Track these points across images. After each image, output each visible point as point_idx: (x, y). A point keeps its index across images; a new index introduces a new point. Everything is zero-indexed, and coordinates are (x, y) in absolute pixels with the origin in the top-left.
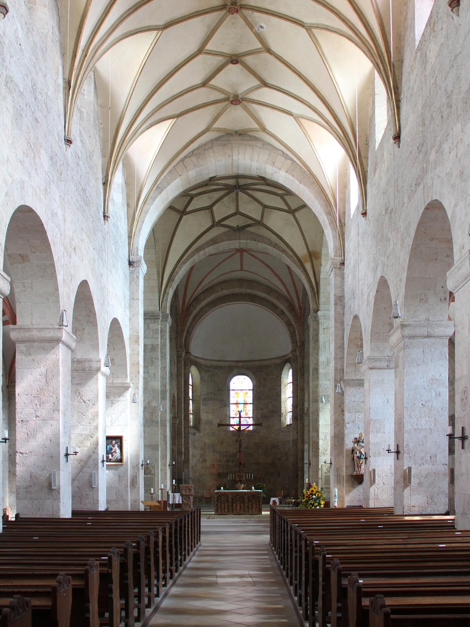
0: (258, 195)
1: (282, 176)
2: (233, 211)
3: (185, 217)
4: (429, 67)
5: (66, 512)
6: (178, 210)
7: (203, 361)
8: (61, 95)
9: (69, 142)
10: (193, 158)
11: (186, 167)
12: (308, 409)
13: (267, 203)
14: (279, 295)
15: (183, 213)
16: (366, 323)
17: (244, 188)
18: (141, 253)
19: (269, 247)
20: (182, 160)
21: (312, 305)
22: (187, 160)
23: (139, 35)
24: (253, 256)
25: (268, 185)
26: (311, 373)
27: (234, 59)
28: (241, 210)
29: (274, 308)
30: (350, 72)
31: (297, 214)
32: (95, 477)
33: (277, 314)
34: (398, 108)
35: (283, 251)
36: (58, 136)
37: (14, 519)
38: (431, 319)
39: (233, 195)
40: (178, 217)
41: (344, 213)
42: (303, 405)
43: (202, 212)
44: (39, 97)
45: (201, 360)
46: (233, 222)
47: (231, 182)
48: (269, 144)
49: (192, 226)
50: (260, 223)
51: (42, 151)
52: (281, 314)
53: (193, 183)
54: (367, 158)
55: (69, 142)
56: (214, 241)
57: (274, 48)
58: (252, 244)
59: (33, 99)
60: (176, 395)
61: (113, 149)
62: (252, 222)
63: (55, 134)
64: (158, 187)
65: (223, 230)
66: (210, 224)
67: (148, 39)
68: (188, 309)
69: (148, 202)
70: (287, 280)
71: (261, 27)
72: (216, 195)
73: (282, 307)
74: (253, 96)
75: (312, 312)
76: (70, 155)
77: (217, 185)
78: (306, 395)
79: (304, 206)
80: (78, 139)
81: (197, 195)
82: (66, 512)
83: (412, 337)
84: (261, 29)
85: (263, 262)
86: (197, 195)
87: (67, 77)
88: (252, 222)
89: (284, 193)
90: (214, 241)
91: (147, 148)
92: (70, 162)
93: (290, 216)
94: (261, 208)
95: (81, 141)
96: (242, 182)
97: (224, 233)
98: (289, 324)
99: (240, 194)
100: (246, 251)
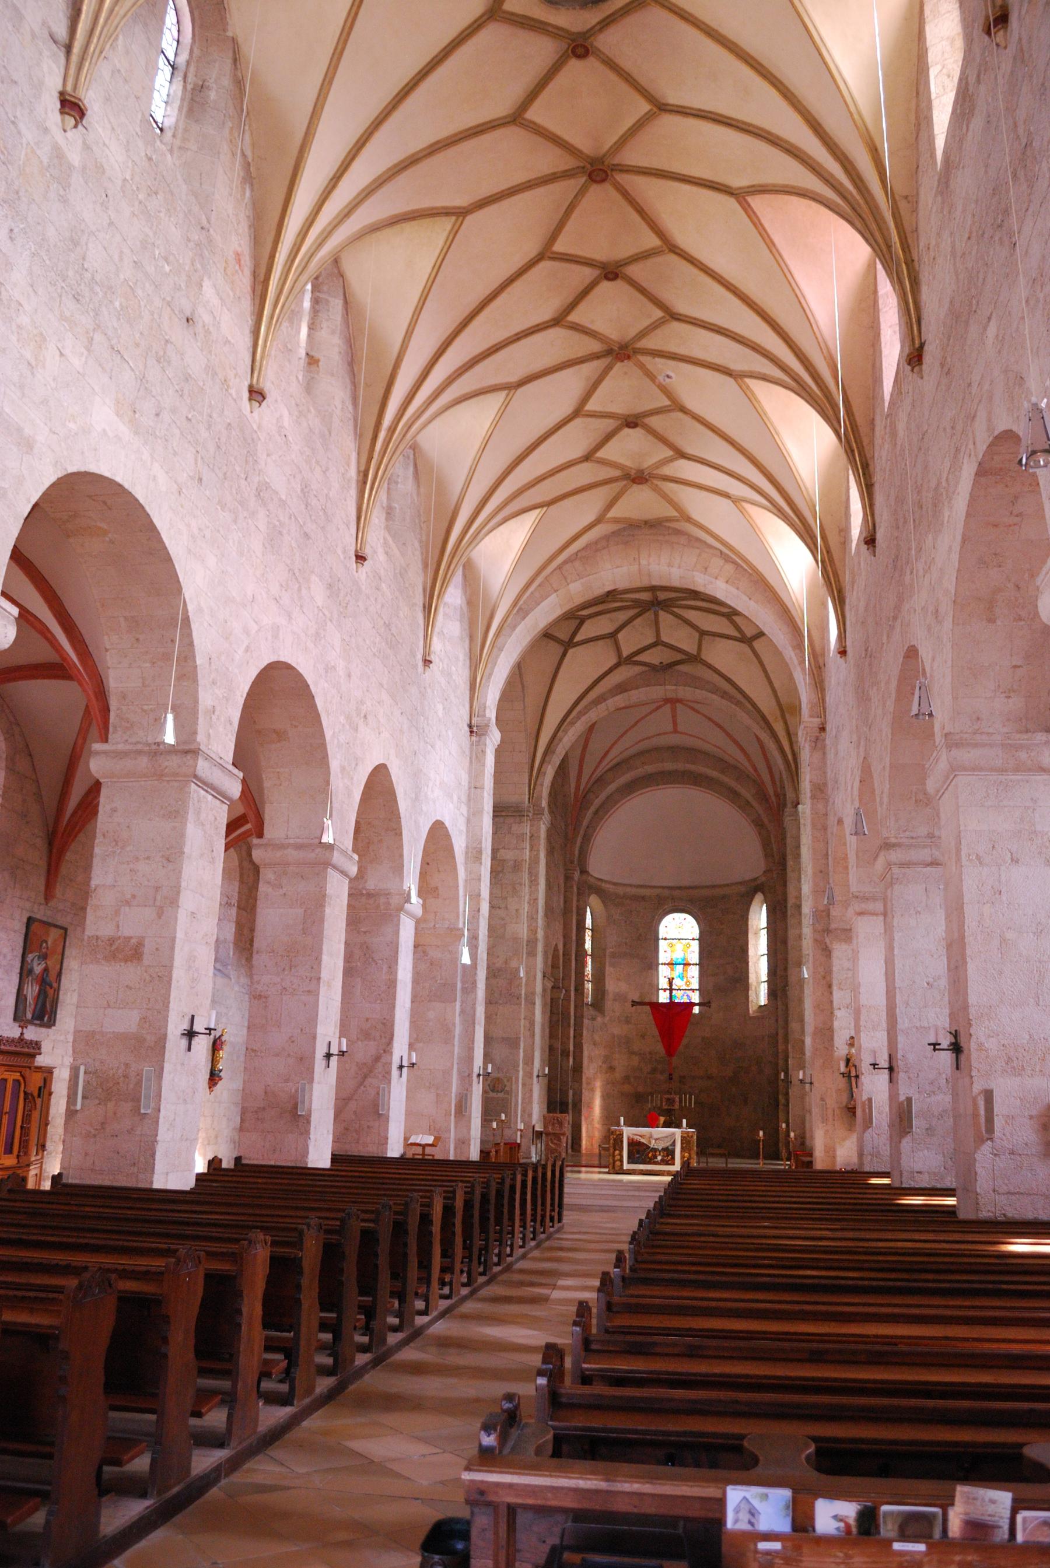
0: (692, 615)
1: (721, 589)
2: (651, 640)
3: (571, 652)
5: (319, 1156)
7: (611, 888)
8: (353, 493)
9: (360, 558)
10: (577, 564)
11: (565, 578)
13: (706, 627)
14: (740, 774)
15: (569, 644)
17: (666, 605)
19: (714, 697)
20: (559, 568)
21: (790, 795)
22: (567, 566)
23: (482, 397)
25: (703, 600)
28: (665, 638)
29: (733, 796)
31: (756, 644)
32: (384, 1095)
33: (739, 807)
37: (232, 1166)
39: (649, 615)
40: (562, 650)
43: (600, 642)
45: (608, 886)
46: (653, 657)
47: (645, 596)
49: (584, 666)
50: (695, 659)
51: (314, 578)
52: (744, 806)
53: (579, 600)
56: (621, 688)
57: (690, 404)
58: (685, 692)
60: (561, 947)
61: (442, 555)
62: (684, 657)
64: (520, 609)
65: (638, 669)
66: (613, 661)
67: (494, 402)
68: (583, 801)
69: (504, 632)
70: (754, 750)
71: (668, 376)
72: (622, 616)
73: (747, 793)
75: (789, 805)
77: (622, 601)
79: (761, 634)
80: (380, 551)
81: (590, 616)
82: (319, 1156)
84: (668, 380)
85: (710, 719)
86: (590, 616)
90: (621, 688)
91: (503, 551)
94: (697, 635)
96: (662, 596)
97: (641, 674)
98: (758, 823)
99: (662, 614)
100: (679, 701)
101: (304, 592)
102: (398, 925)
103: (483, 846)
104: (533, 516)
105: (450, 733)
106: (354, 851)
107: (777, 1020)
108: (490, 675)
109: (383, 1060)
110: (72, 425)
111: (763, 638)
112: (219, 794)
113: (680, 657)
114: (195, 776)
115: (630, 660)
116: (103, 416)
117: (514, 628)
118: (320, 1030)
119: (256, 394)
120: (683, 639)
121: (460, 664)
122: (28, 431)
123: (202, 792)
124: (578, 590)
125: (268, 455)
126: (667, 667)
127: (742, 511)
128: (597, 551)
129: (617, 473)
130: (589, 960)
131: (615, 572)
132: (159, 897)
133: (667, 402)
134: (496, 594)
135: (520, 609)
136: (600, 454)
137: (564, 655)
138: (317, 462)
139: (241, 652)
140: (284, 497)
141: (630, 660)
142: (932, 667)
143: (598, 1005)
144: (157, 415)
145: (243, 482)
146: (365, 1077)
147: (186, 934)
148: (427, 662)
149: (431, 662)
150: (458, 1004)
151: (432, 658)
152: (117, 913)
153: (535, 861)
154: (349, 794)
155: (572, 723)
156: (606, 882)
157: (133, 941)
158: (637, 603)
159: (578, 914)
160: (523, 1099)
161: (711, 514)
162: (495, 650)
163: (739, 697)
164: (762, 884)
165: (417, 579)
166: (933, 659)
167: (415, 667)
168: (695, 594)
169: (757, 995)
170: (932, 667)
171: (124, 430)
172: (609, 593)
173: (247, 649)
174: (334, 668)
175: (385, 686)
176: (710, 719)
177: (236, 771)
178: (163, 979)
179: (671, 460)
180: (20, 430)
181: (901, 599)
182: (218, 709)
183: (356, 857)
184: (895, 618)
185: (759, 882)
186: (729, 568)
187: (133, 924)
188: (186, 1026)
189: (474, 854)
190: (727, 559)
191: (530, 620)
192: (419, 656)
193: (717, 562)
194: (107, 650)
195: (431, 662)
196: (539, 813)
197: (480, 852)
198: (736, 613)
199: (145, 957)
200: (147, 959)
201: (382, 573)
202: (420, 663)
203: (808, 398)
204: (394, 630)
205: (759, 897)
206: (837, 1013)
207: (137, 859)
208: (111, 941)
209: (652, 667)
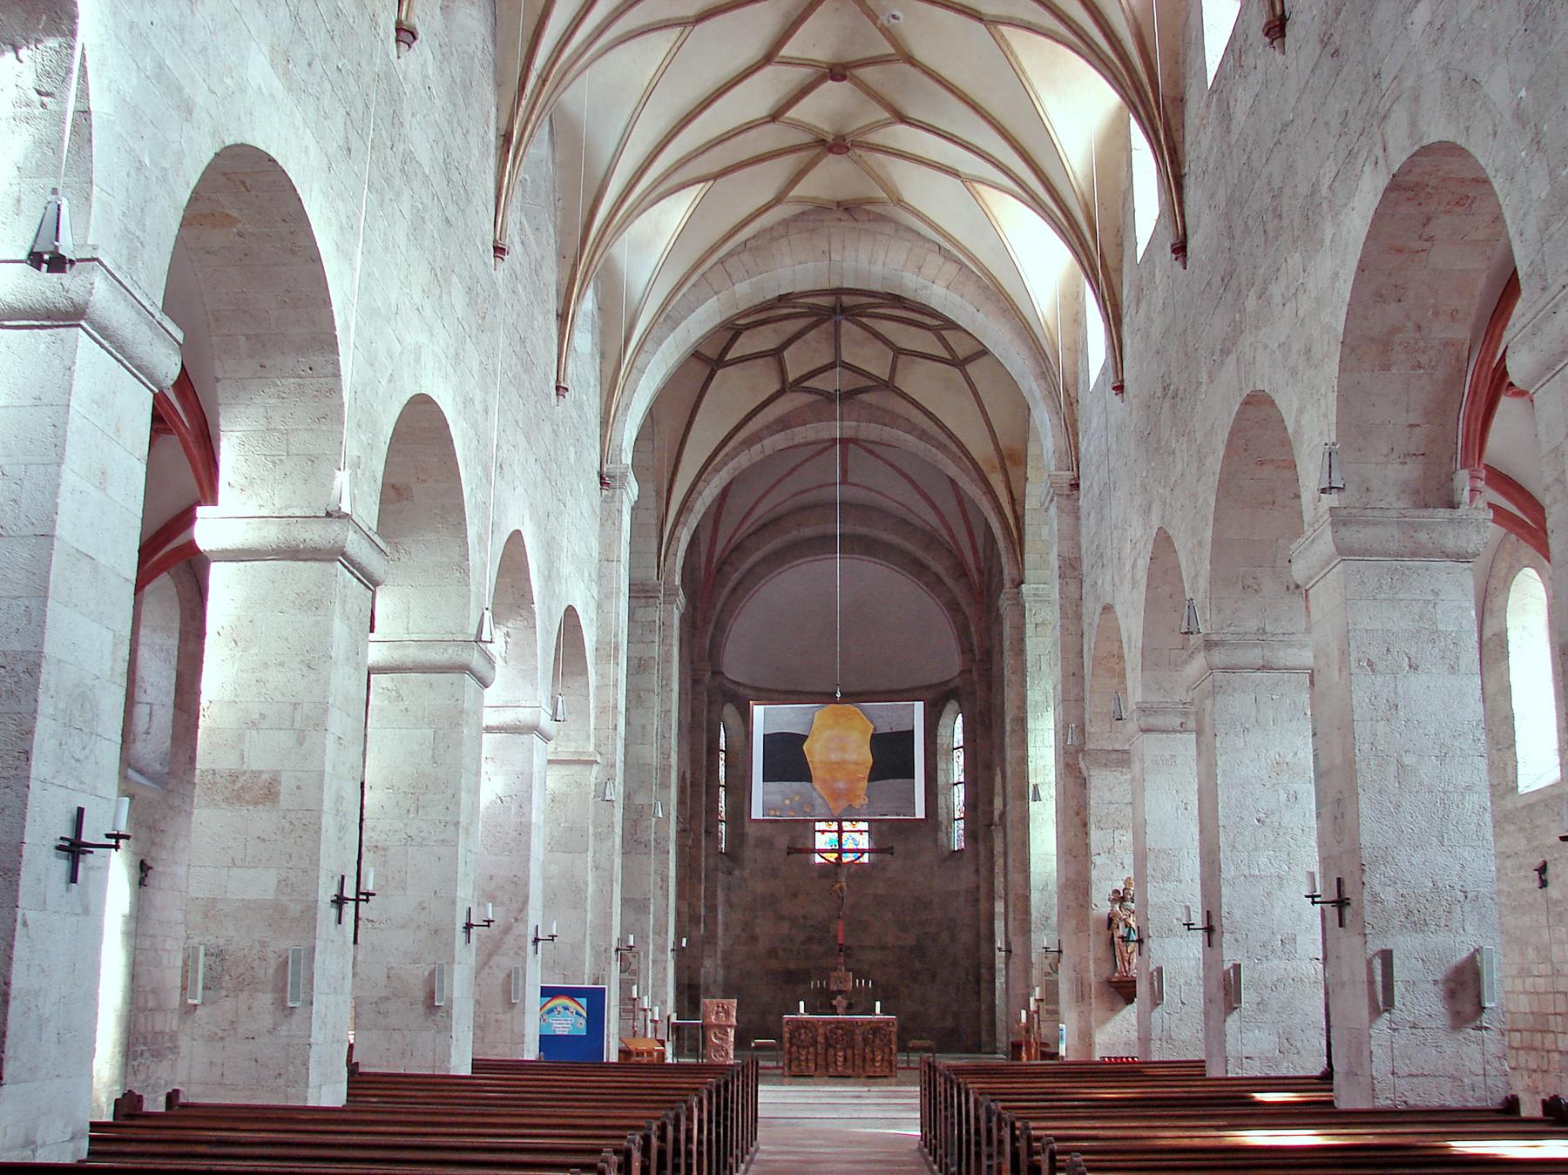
0: (884, 327)
1: (939, 293)
2: (827, 359)
4: (1235, 131)
6: (708, 361)
10: (746, 257)
12: (1003, 814)
14: (931, 540)
16: (1132, 625)
19: (909, 437)
22: (731, 261)
24: (870, 452)
26: (1008, 728)
27: (837, 72)
28: (846, 358)
29: (918, 568)
30: (1077, 107)
31: (969, 368)
33: (926, 584)
34: (1180, 187)
35: (940, 446)
38: (1268, 629)
41: (1076, 380)
42: (991, 802)
43: (760, 361)
48: (909, 229)
50: (888, 386)
52: (935, 584)
53: (743, 306)
54: (1119, 271)
56: (784, 424)
57: (920, 54)
58: (870, 431)
62: (870, 383)
64: (667, 317)
65: (805, 398)
66: (776, 387)
67: (662, 42)
70: (950, 507)
73: (938, 566)
74: (876, 138)
75: (1007, 584)
78: (998, 779)
81: (748, 327)
83: (1226, 669)
85: (892, 465)
86: (748, 327)
88: (870, 383)
89: (943, 325)
90: (784, 424)
93: (956, 372)
96: (847, 300)
97: (809, 405)
98: (954, 608)
100: (854, 441)
101: (445, 297)
104: (693, 192)
107: (977, 871)
108: (628, 405)
109: (515, 931)
111: (985, 359)
113: (864, 382)
115: (797, 385)
118: (461, 893)
119: (406, 34)
120: (874, 361)
124: (745, 291)
126: (849, 395)
127: (975, 196)
128: (773, 239)
129: (805, 138)
130: (722, 791)
131: (797, 270)
132: (298, 718)
133: (889, 49)
134: (638, 296)
135: (668, 316)
136: (792, 113)
137: (710, 378)
141: (797, 385)
142: (1298, 422)
143: (733, 856)
146: (490, 955)
150: (590, 854)
153: (668, 660)
155: (717, 470)
156: (745, 686)
157: (265, 776)
158: (811, 307)
159: (709, 730)
160: (654, 981)
161: (929, 196)
162: (634, 371)
163: (943, 438)
164: (957, 688)
165: (551, 276)
166: (1301, 411)
167: (548, 396)
168: (897, 300)
169: (949, 835)
170: (1298, 422)
171: (278, 86)
172: (781, 298)
176: (892, 465)
179: (887, 124)
181: (1237, 329)
182: (363, 460)
184: (1225, 352)
185: (952, 685)
186: (951, 268)
188: (334, 891)
189: (607, 651)
190: (948, 256)
191: (680, 332)
192: (553, 384)
193: (935, 260)
194: (217, 380)
196: (670, 594)
198: (951, 325)
199: (282, 797)
200: (285, 801)
203: (1096, 62)
205: (952, 706)
206: (1096, 859)
208: (234, 777)
209: (829, 397)
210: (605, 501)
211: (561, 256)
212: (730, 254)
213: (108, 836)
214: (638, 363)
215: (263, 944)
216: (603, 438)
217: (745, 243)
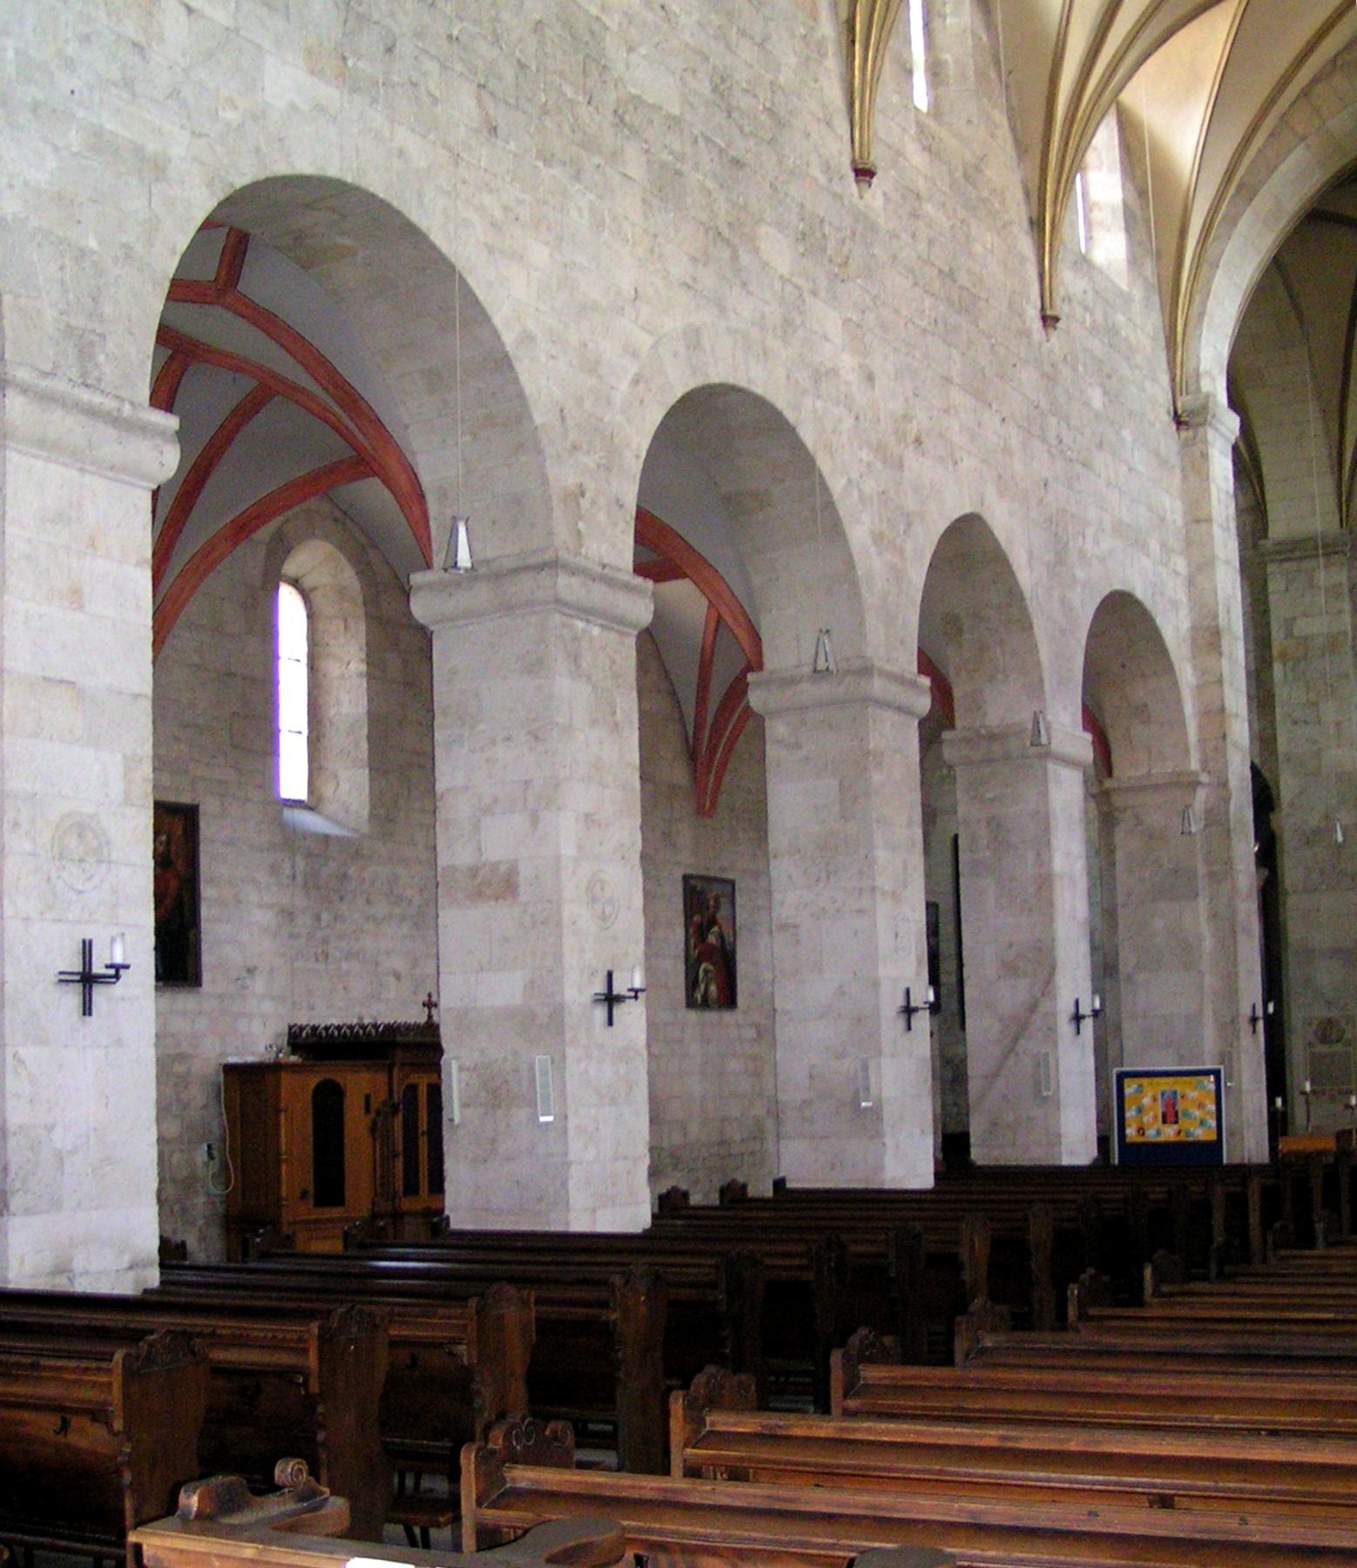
18: (1216, 387)
20: (1305, 93)
22: (1319, 88)
36: (827, 168)
44: (744, 102)
55: (864, 173)
59: (720, 118)
63: (815, 171)
64: (1237, 185)
76: (879, 202)
87: (844, 15)
92: (881, 221)
95: (928, 149)
101: (745, 258)
102: (1045, 782)
103: (1222, 621)
105: (1126, 434)
106: (921, 671)
108: (1202, 314)
110: (231, 116)
112: (613, 621)
114: (557, 601)
116: (285, 81)
117: (1232, 221)
121: (1136, 308)
122: (151, 147)
123: (580, 625)
125: (630, 50)
132: (530, 799)
135: (1241, 186)
138: (742, 33)
139: (624, 386)
140: (676, 111)
144: (389, 50)
145: (584, 112)
147: (580, 848)
148: (1049, 321)
149: (1057, 319)
151: (1061, 309)
152: (477, 827)
154: (898, 575)
157: (503, 868)
162: (1205, 269)
165: (1006, 176)
167: (1025, 333)
171: (328, 93)
173: (636, 381)
174: (834, 372)
175: (957, 380)
177: (639, 580)
178: (549, 922)
180: (138, 150)
183: (926, 681)
187: (500, 841)
189: (1208, 638)
191: (1262, 202)
192: (1033, 314)
194: (407, 427)
195: (1057, 319)
197: (1216, 633)
199: (522, 890)
200: (525, 893)
201: (922, 185)
202: (1037, 324)
204: (962, 278)
207: (493, 742)
210: (1186, 445)
211: (1021, 148)
212: (1315, 81)
213: (107, 967)
214: (1210, 254)
215: (516, 1054)
216: (1171, 363)
217: (1334, 60)
